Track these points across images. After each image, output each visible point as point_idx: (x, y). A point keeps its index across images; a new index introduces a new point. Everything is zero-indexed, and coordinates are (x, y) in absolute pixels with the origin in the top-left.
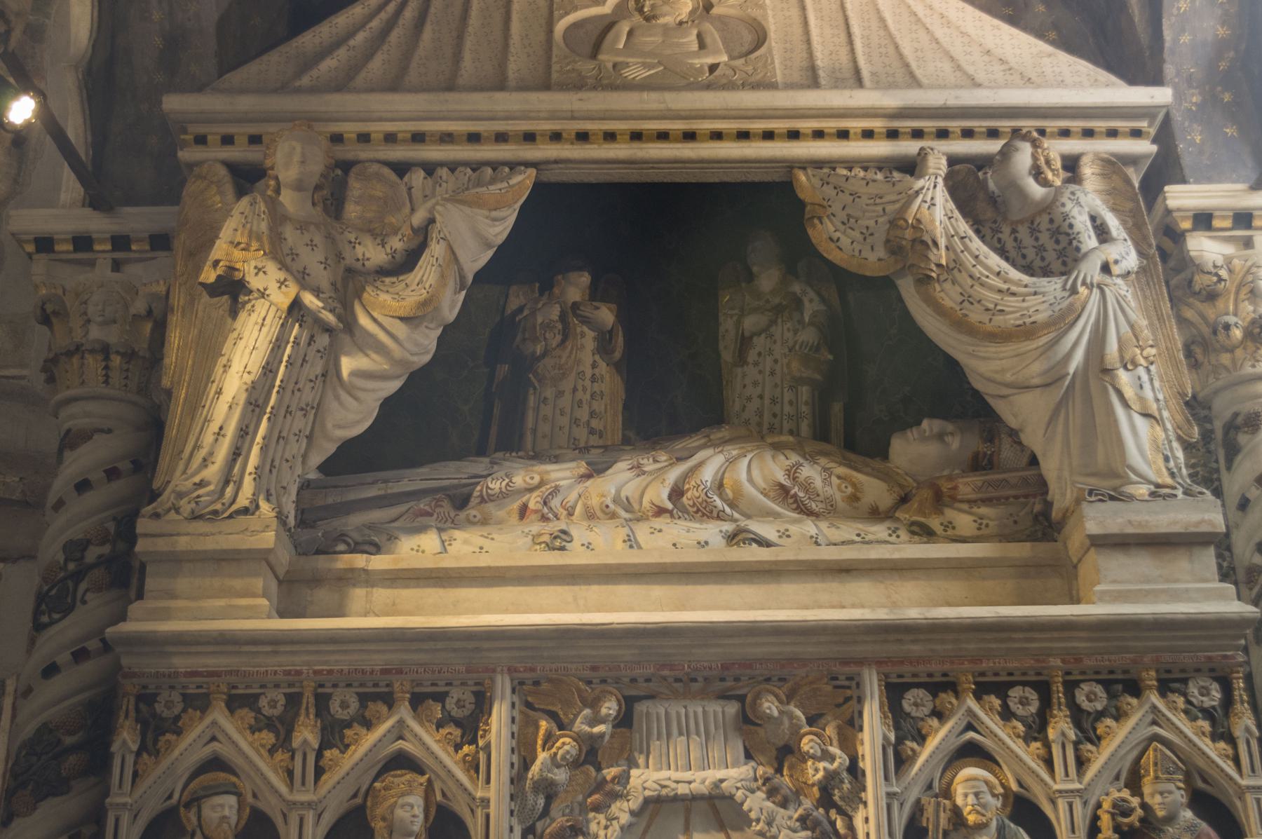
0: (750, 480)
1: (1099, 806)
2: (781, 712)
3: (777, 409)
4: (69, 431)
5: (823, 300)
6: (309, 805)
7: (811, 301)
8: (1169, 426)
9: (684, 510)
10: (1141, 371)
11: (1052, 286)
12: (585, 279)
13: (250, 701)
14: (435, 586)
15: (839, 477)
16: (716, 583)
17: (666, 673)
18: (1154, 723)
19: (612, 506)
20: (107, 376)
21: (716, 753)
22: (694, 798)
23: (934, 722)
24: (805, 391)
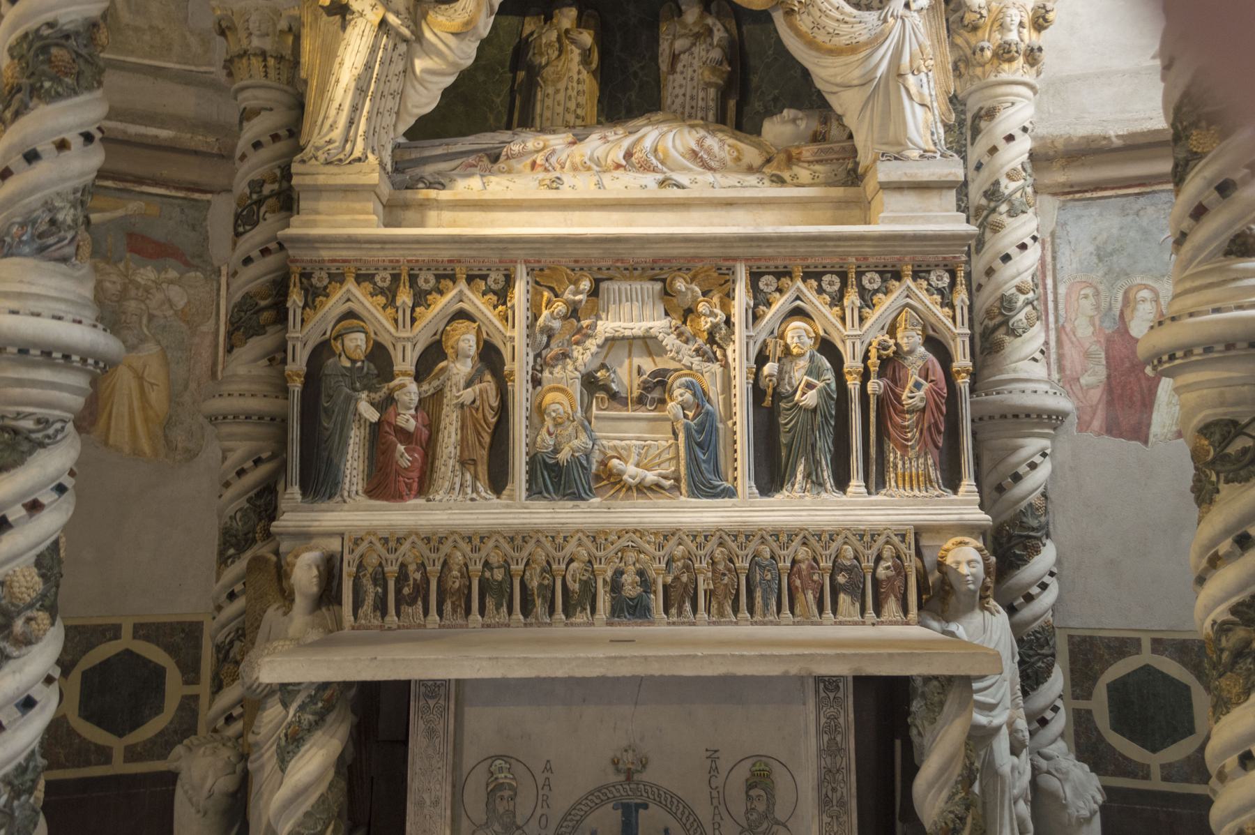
0: (674, 147)
1: (870, 344)
2: (687, 289)
3: (694, 103)
4: (245, 109)
5: (727, 30)
6: (408, 339)
7: (719, 30)
8: (936, 112)
9: (633, 166)
10: (923, 76)
11: (871, 17)
12: (573, 12)
13: (370, 278)
14: (479, 210)
15: (729, 146)
16: (651, 211)
17: (619, 264)
18: (907, 296)
19: (588, 163)
20: (266, 72)
21: (648, 311)
22: (634, 338)
23: (777, 295)
24: (712, 91)
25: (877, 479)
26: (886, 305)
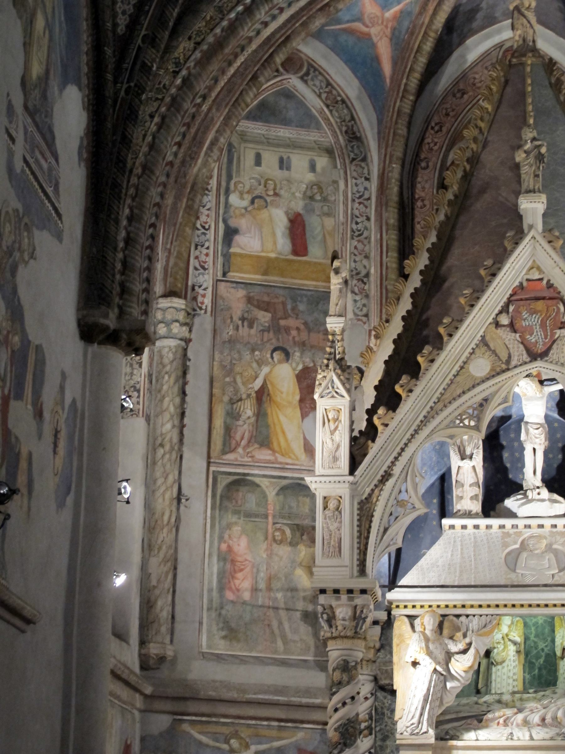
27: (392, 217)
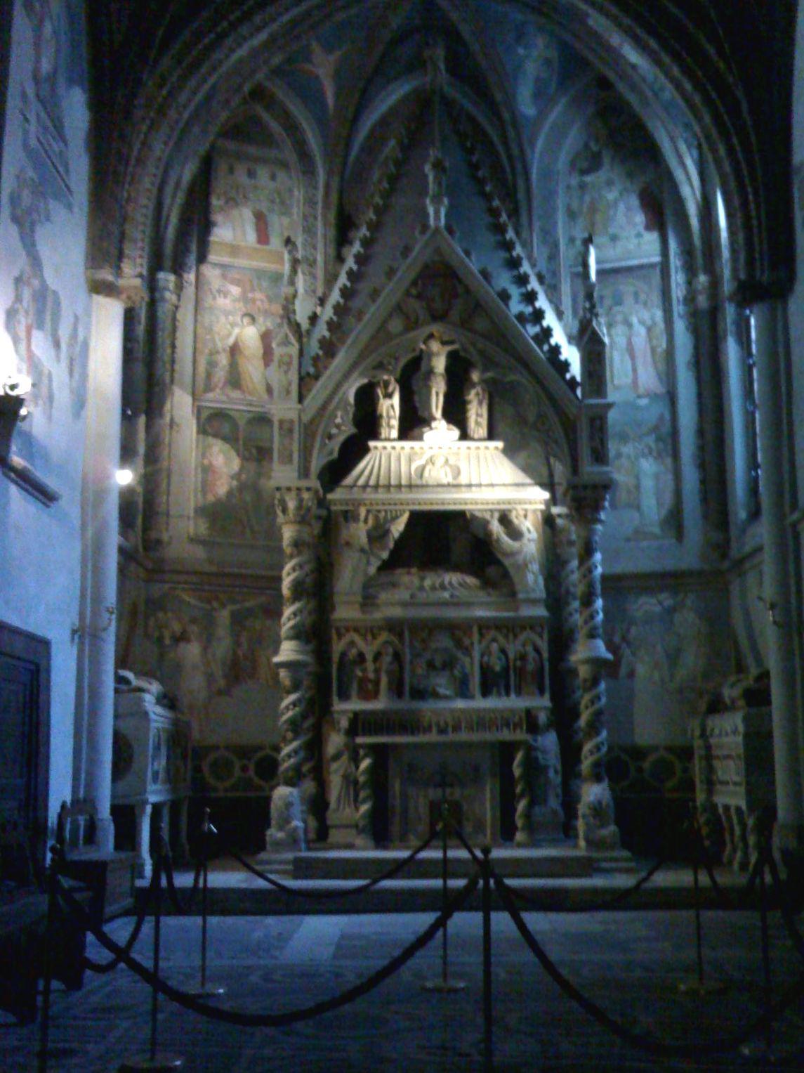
25: (519, 693)
26: (523, 637)
27: (332, 216)
